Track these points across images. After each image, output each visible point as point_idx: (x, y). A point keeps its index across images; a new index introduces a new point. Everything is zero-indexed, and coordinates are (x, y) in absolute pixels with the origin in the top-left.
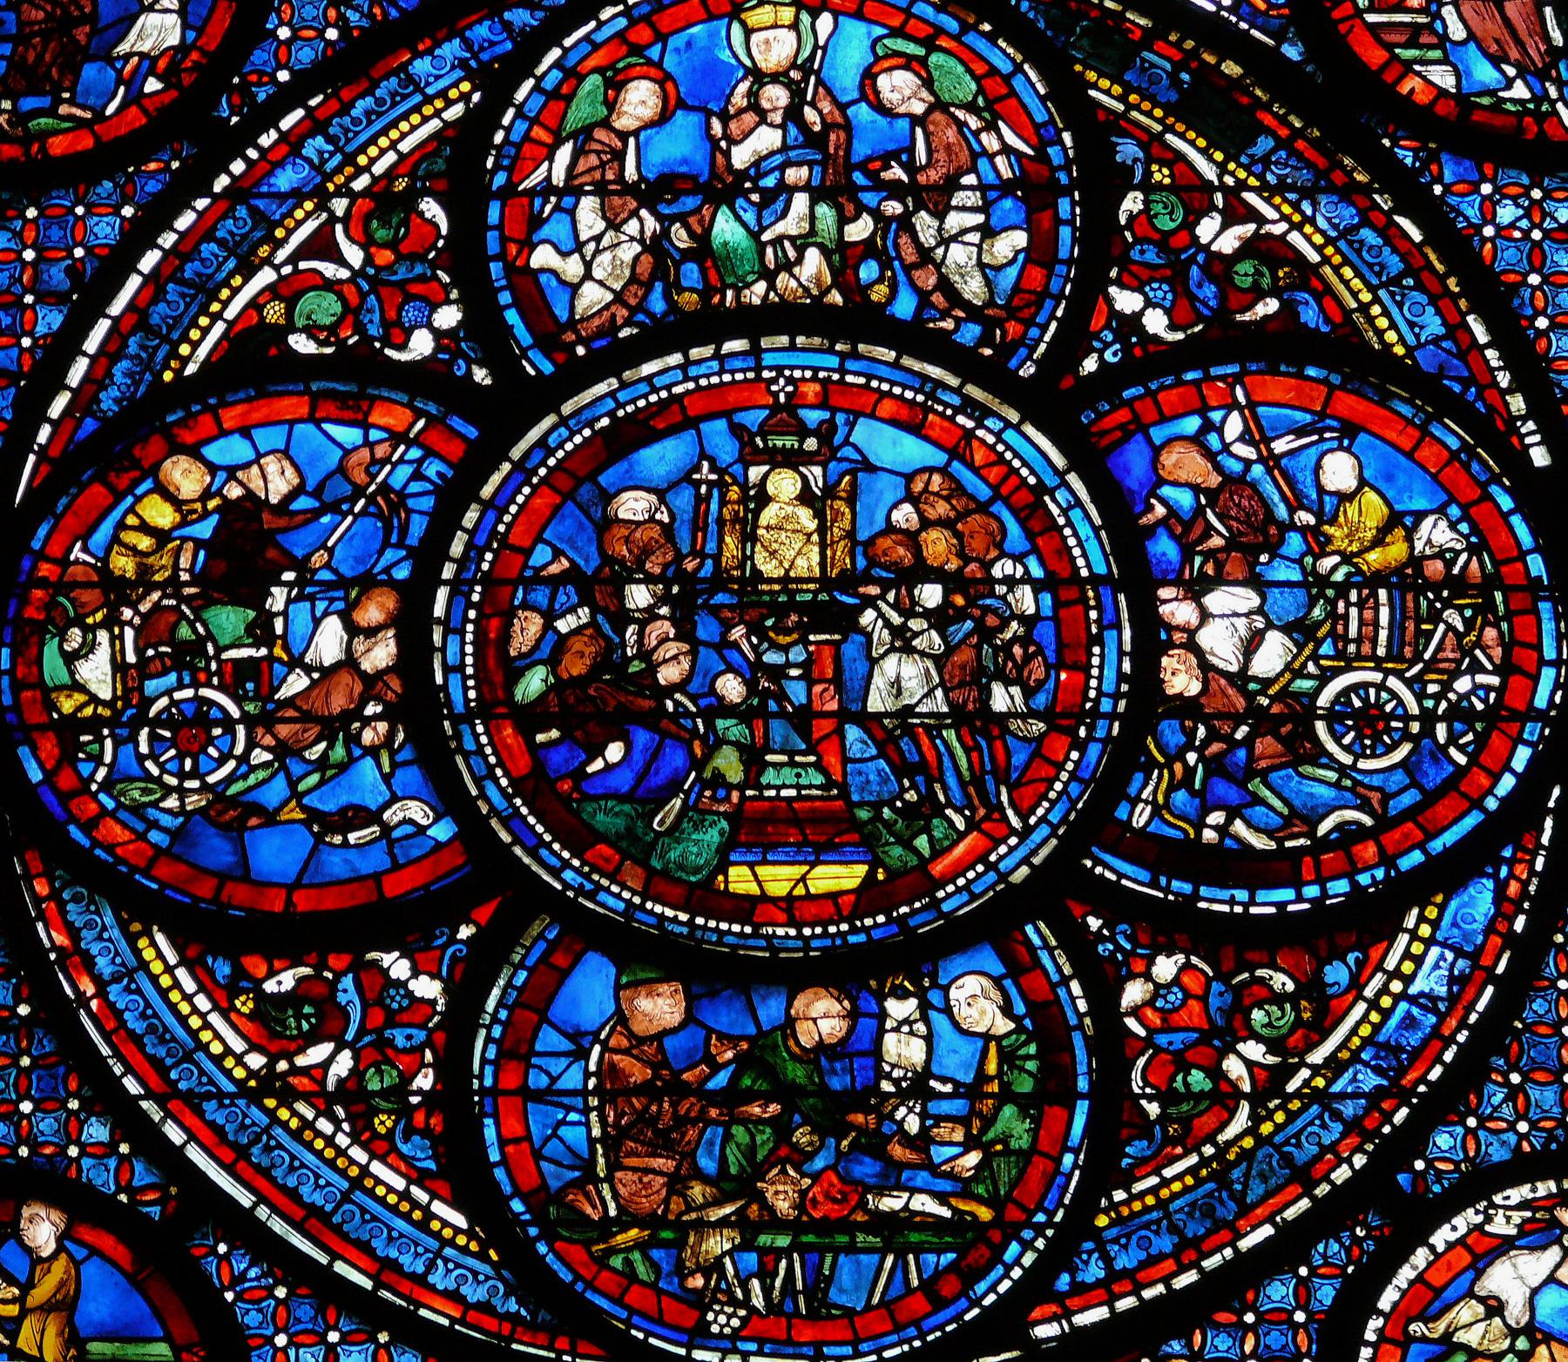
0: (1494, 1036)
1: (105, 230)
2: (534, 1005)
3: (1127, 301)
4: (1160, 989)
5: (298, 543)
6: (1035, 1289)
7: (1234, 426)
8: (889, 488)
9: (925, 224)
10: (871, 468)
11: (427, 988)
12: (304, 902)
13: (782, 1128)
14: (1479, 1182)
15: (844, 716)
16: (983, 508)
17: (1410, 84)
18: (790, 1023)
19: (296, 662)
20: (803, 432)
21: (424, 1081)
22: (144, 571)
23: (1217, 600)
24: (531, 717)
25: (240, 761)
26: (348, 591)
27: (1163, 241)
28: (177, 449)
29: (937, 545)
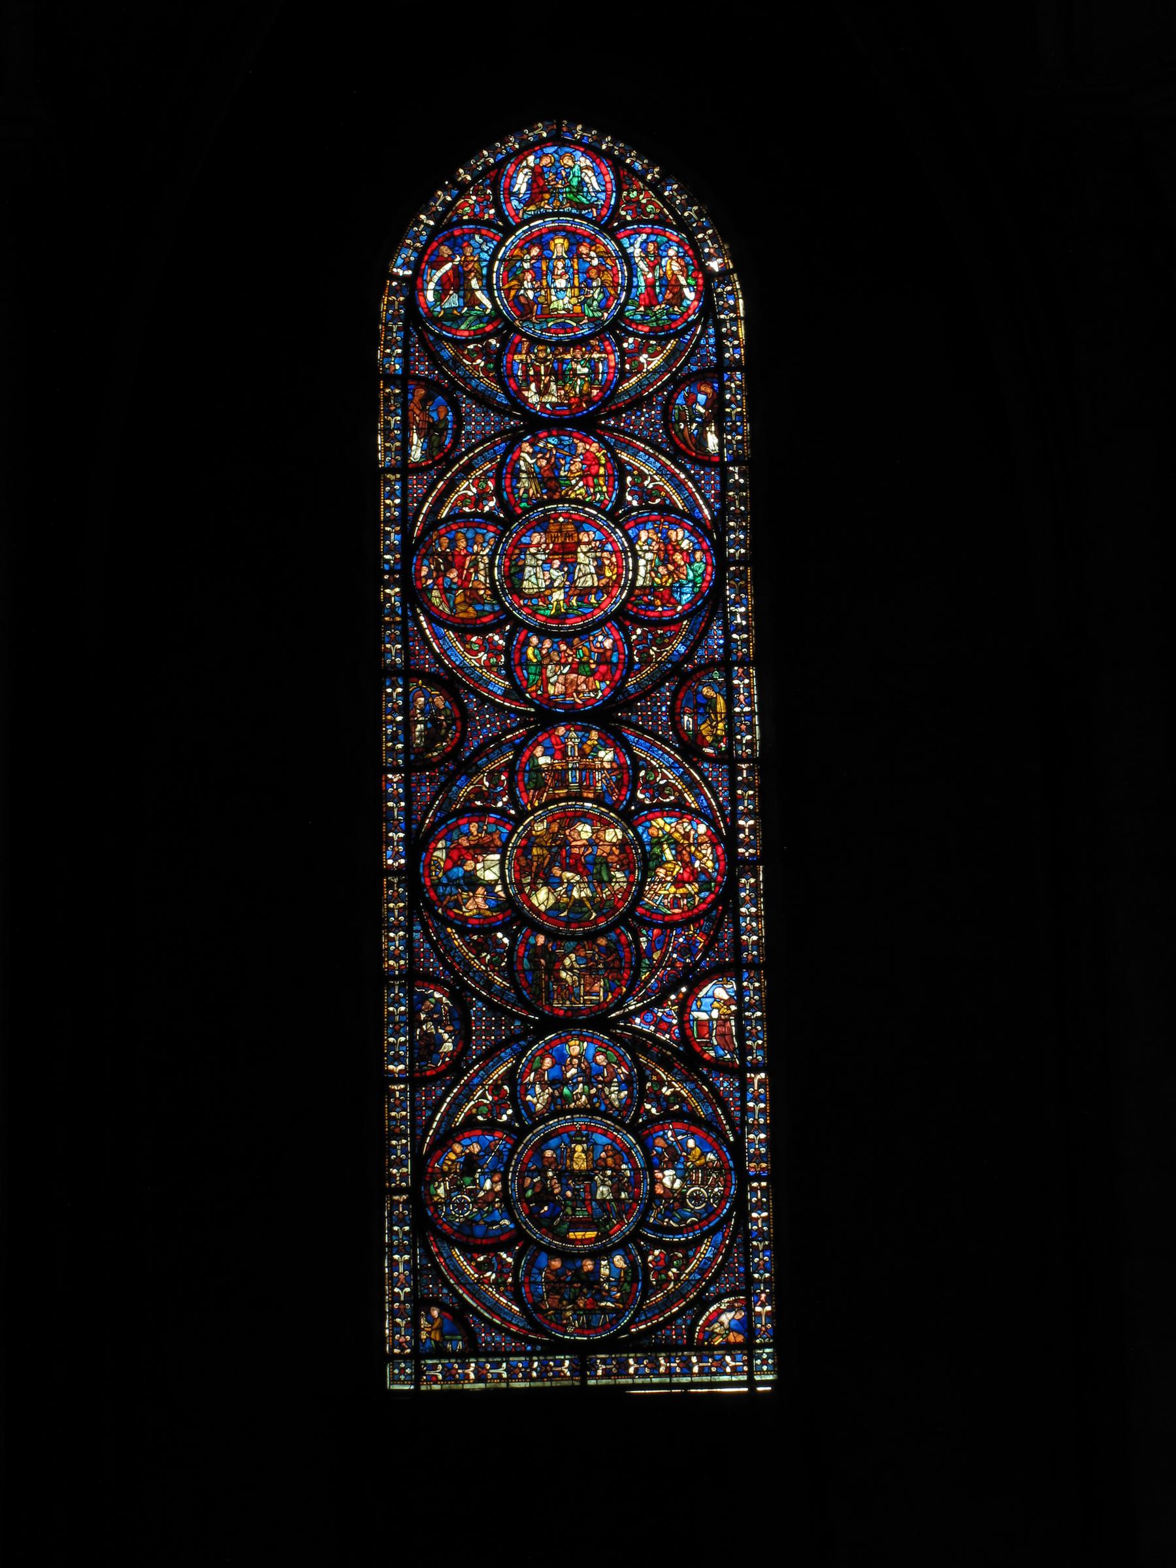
0: (722, 1266)
1: (439, 1092)
2: (531, 1264)
3: (648, 1106)
4: (656, 1257)
5: (481, 1162)
6: (632, 1322)
7: (670, 1133)
8: (600, 1148)
9: (606, 1089)
10: (595, 1144)
11: (510, 1260)
12: (484, 1241)
13: (581, 1289)
14: (718, 1298)
15: (591, 1200)
16: (618, 1153)
17: (706, 1056)
18: (582, 1267)
19: (481, 1189)
20: (582, 1136)
21: (510, 1280)
22: (450, 1169)
23: (667, 1173)
24: (528, 1201)
25: (471, 1211)
26: (490, 1174)
27: (655, 1093)
28: (455, 1142)
29: (610, 1161)
